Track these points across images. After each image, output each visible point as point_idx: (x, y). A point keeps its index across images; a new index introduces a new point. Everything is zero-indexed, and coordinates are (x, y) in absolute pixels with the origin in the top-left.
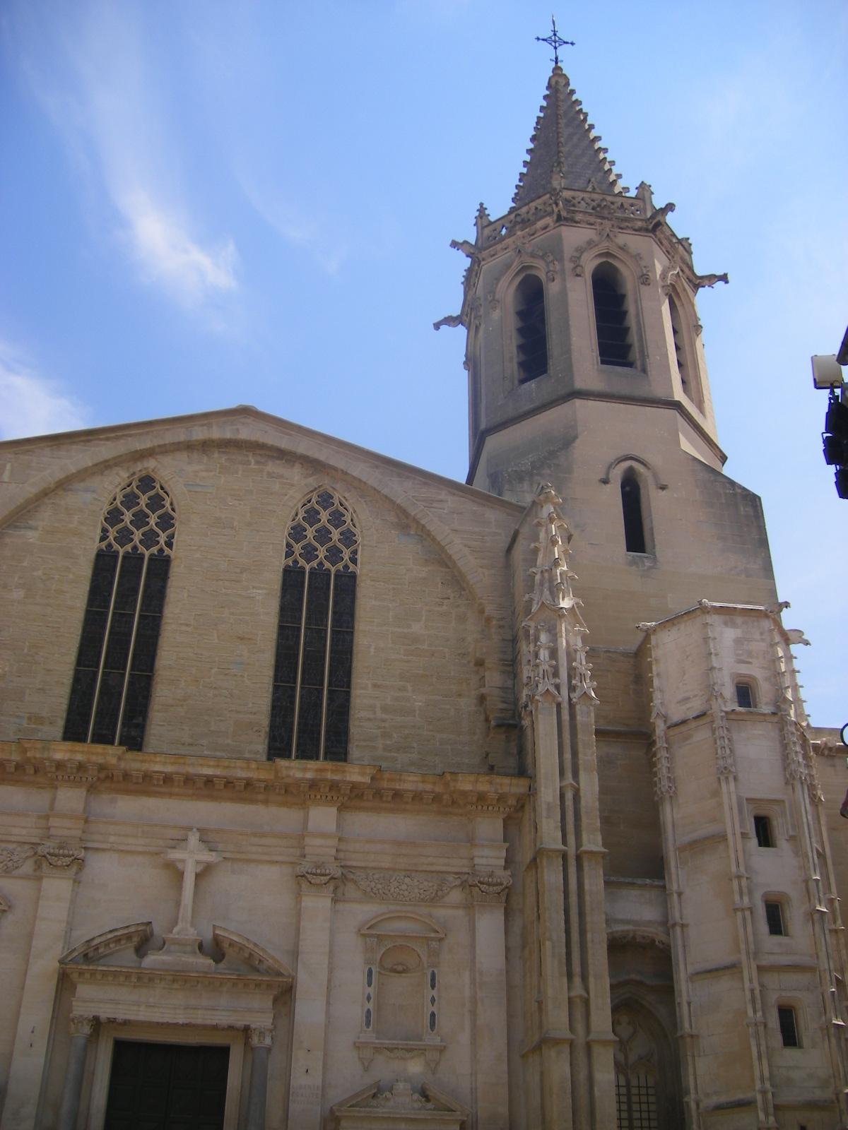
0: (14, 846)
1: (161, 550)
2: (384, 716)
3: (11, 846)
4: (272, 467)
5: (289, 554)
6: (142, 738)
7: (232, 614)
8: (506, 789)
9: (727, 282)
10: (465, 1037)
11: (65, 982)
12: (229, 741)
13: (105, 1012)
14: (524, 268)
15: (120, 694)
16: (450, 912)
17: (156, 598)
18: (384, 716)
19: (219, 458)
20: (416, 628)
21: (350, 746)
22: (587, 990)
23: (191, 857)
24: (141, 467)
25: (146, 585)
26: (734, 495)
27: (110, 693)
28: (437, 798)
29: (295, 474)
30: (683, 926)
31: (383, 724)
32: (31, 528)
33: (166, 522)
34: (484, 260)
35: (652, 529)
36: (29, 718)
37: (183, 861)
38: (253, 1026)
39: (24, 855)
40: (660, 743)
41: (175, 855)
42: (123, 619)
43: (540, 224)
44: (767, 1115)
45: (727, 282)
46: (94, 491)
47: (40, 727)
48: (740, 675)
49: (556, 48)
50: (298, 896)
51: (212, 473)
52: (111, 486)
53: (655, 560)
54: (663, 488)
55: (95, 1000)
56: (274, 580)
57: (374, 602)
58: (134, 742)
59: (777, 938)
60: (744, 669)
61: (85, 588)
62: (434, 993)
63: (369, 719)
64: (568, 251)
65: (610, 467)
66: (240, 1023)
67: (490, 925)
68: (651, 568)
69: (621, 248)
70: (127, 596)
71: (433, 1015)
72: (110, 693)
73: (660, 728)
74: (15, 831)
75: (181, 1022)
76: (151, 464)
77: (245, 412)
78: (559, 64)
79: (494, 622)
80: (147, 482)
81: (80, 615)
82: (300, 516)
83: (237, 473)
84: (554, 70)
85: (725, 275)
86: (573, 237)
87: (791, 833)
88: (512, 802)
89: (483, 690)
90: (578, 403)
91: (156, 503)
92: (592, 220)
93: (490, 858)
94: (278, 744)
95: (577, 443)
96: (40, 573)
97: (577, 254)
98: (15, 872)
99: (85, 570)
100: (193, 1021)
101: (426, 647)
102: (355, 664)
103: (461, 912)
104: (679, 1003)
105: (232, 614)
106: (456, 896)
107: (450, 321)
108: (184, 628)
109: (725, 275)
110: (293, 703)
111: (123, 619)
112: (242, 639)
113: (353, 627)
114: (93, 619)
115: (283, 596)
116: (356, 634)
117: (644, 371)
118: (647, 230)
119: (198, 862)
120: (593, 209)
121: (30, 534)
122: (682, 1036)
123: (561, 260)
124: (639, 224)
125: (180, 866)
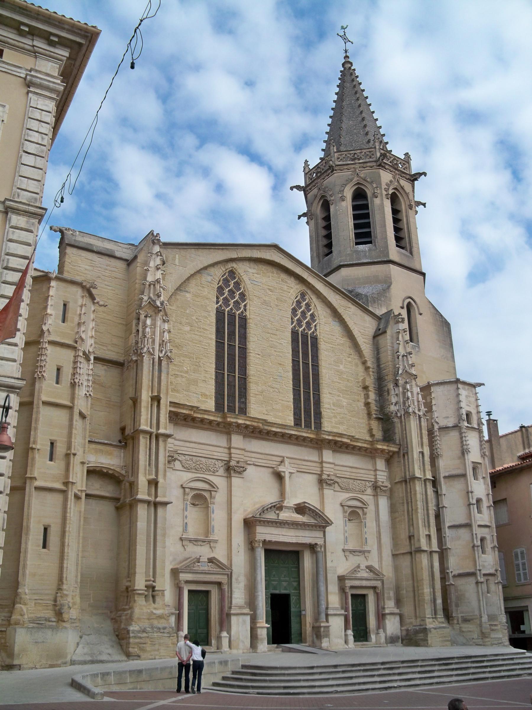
0: (215, 460)
1: (242, 312)
2: (334, 408)
3: (213, 461)
4: (283, 276)
5: (292, 323)
6: (246, 409)
7: (275, 351)
8: (392, 449)
9: (425, 207)
10: (375, 547)
11: (249, 524)
12: (280, 414)
13: (268, 538)
14: (358, 183)
15: (235, 386)
16: (368, 497)
17: (244, 337)
18: (334, 408)
19: (263, 268)
20: (341, 367)
21: (322, 420)
22: (429, 531)
23: (286, 469)
24: (230, 266)
25: (239, 331)
26: (442, 321)
27: (231, 385)
28: (366, 449)
29: (291, 282)
30: (446, 507)
31: (333, 411)
32: (187, 292)
33: (243, 296)
34: (336, 170)
35: (417, 333)
36: (202, 395)
37: (284, 472)
38: (319, 543)
39: (220, 466)
40: (437, 433)
41: (281, 469)
42: (231, 347)
43: (368, 164)
44: (481, 578)
45: (425, 207)
46: (211, 276)
47: (207, 400)
48: (467, 411)
49: (345, 43)
50: (321, 489)
51: (259, 276)
52: (218, 273)
53: (419, 347)
54: (421, 314)
55: (264, 533)
56: (289, 335)
57: (326, 353)
58: (243, 411)
59: (479, 515)
60: (468, 409)
61: (213, 329)
62: (366, 530)
63: (329, 409)
64: (384, 186)
65: (404, 301)
66: (313, 543)
67: (383, 502)
68: (418, 351)
69: (401, 187)
70: (232, 334)
71: (366, 538)
72: (231, 385)
73: (436, 427)
74: (216, 454)
75: (294, 542)
76: (234, 265)
77: (276, 247)
78: (348, 54)
79: (371, 370)
80: (232, 273)
81: (214, 343)
82: (294, 304)
83: (269, 277)
84: (345, 58)
85: (425, 203)
86: (386, 176)
87: (484, 476)
88: (391, 454)
89: (370, 401)
90: (391, 266)
91: (237, 285)
92: (392, 170)
93: (382, 477)
94: (296, 417)
95: (392, 287)
96: (194, 318)
97: (386, 187)
98: (217, 474)
99: (213, 319)
100: (298, 542)
101: (345, 377)
102: (321, 381)
103: (371, 497)
104: (444, 537)
105: (275, 351)
106: (369, 491)
107: (298, 187)
108: (257, 356)
109: (425, 203)
110: (300, 397)
111: (231, 347)
112: (281, 364)
113: (318, 363)
114: (219, 345)
115: (292, 345)
116: (320, 367)
117: (411, 253)
118: (410, 180)
119: (290, 473)
120: (390, 162)
121: (188, 295)
122: (446, 549)
123: (381, 188)
124: (408, 177)
125: (283, 474)
